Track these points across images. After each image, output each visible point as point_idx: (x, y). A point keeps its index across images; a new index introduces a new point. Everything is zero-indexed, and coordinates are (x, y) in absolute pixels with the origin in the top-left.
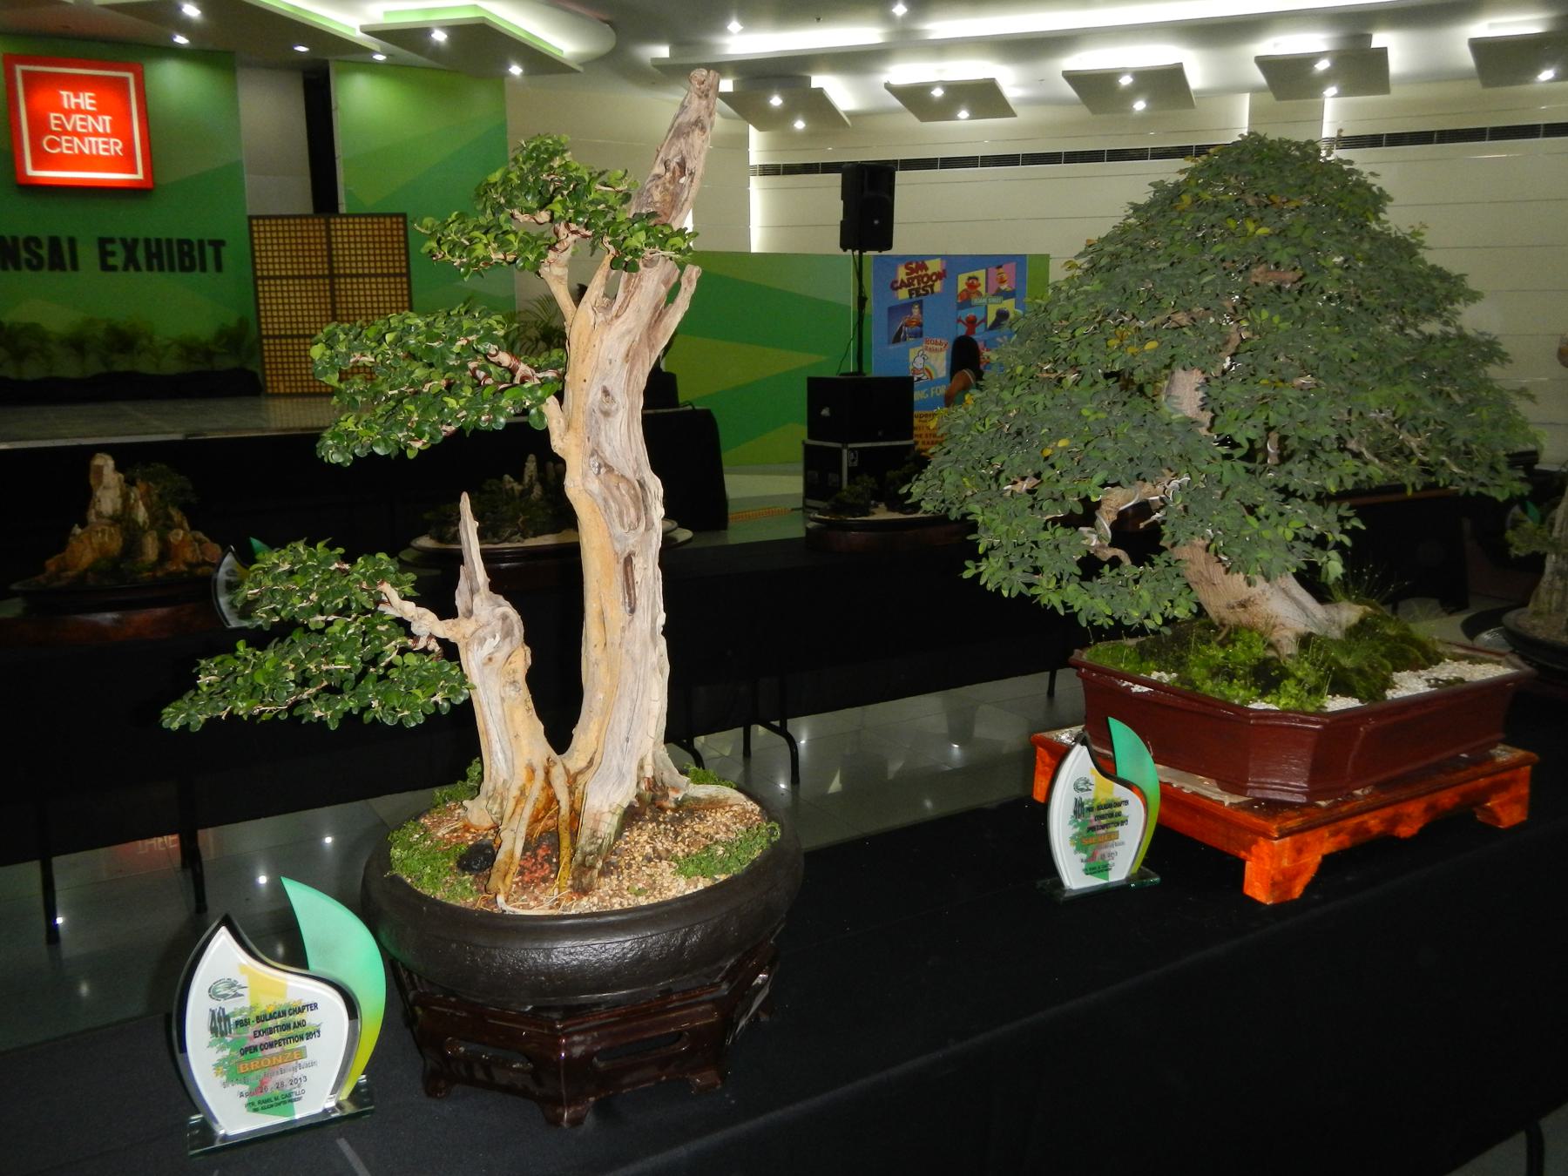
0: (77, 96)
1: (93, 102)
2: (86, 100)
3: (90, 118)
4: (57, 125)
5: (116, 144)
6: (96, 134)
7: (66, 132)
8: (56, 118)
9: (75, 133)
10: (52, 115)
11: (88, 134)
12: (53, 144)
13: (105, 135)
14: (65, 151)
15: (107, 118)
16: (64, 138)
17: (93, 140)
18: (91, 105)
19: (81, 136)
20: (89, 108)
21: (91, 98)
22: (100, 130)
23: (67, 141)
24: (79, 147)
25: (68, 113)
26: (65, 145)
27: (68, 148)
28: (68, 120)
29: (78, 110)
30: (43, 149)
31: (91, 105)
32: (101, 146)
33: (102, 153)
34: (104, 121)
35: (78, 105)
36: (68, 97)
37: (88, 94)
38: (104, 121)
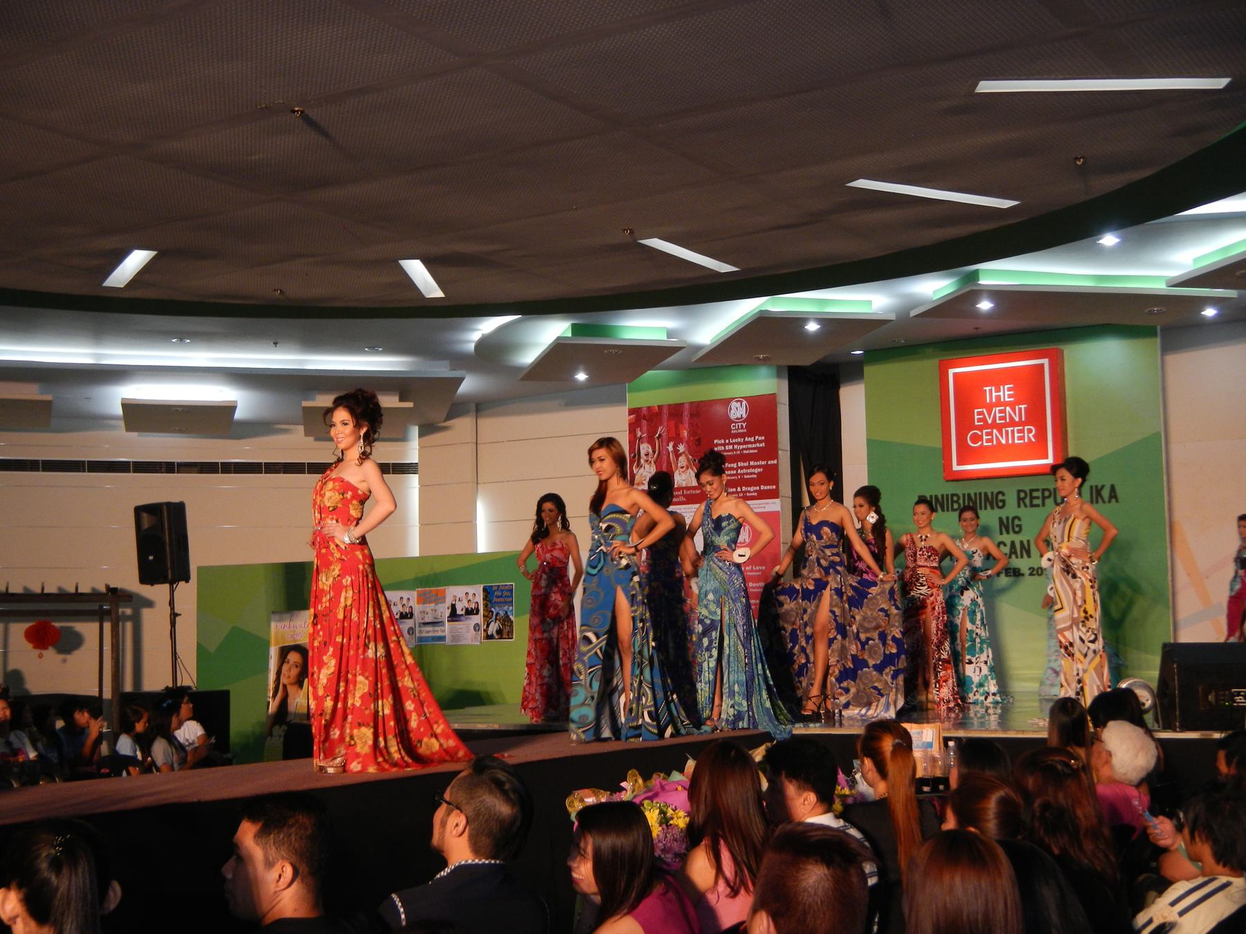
0: (998, 390)
1: (1012, 392)
2: (1005, 393)
3: (1008, 409)
4: (979, 420)
5: (1030, 431)
6: (1013, 423)
7: (986, 426)
8: (979, 413)
9: (994, 425)
10: (976, 411)
11: (1007, 425)
12: (976, 438)
13: (1020, 423)
14: (985, 444)
15: (1023, 407)
16: (984, 431)
17: (1010, 429)
18: (1010, 396)
19: (1000, 428)
20: (1007, 399)
21: (1009, 389)
22: (1017, 419)
23: (987, 434)
24: (997, 438)
25: (989, 408)
26: (985, 437)
27: (988, 441)
28: (989, 415)
29: (999, 403)
30: (970, 446)
31: (1010, 396)
32: (1016, 435)
33: (1016, 441)
34: (1020, 410)
35: (998, 397)
36: (991, 391)
37: (1006, 387)
38: (1020, 410)
